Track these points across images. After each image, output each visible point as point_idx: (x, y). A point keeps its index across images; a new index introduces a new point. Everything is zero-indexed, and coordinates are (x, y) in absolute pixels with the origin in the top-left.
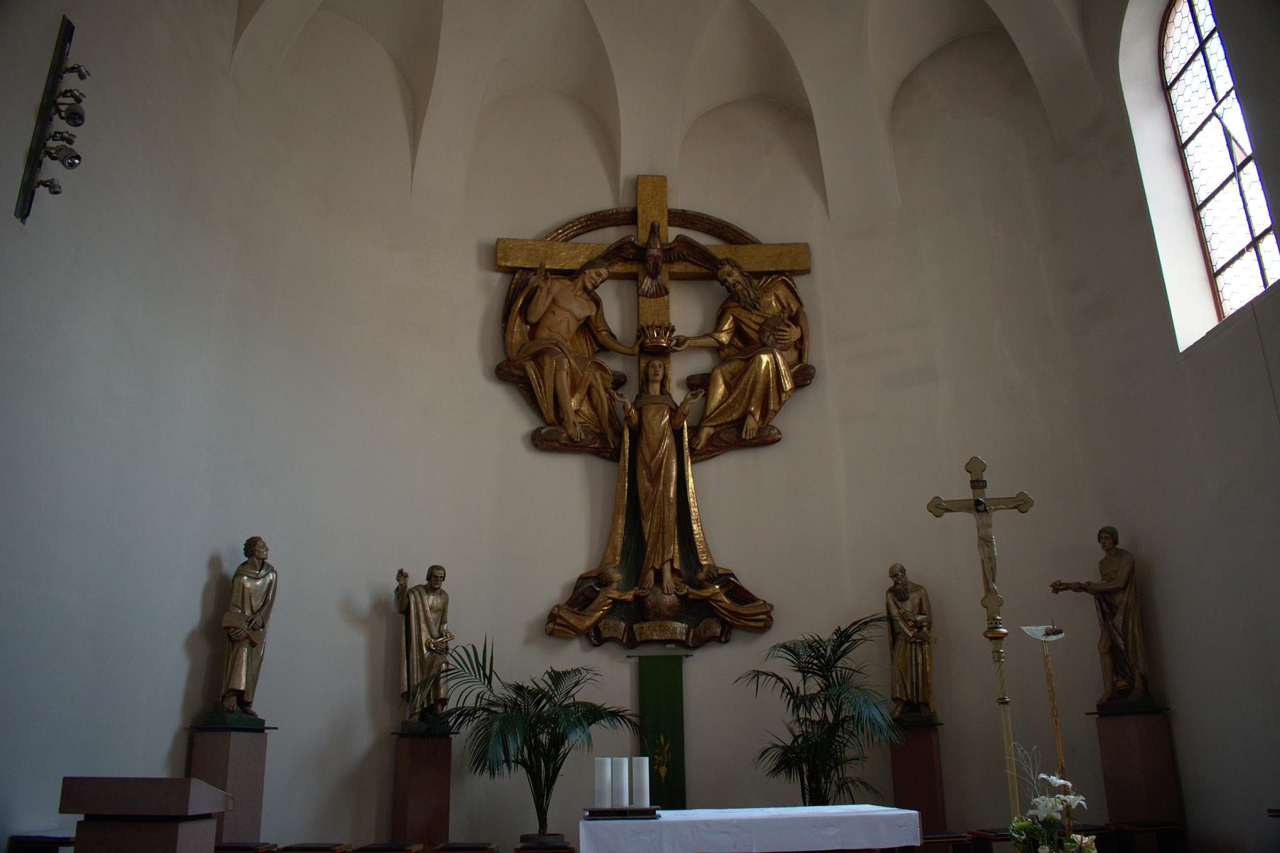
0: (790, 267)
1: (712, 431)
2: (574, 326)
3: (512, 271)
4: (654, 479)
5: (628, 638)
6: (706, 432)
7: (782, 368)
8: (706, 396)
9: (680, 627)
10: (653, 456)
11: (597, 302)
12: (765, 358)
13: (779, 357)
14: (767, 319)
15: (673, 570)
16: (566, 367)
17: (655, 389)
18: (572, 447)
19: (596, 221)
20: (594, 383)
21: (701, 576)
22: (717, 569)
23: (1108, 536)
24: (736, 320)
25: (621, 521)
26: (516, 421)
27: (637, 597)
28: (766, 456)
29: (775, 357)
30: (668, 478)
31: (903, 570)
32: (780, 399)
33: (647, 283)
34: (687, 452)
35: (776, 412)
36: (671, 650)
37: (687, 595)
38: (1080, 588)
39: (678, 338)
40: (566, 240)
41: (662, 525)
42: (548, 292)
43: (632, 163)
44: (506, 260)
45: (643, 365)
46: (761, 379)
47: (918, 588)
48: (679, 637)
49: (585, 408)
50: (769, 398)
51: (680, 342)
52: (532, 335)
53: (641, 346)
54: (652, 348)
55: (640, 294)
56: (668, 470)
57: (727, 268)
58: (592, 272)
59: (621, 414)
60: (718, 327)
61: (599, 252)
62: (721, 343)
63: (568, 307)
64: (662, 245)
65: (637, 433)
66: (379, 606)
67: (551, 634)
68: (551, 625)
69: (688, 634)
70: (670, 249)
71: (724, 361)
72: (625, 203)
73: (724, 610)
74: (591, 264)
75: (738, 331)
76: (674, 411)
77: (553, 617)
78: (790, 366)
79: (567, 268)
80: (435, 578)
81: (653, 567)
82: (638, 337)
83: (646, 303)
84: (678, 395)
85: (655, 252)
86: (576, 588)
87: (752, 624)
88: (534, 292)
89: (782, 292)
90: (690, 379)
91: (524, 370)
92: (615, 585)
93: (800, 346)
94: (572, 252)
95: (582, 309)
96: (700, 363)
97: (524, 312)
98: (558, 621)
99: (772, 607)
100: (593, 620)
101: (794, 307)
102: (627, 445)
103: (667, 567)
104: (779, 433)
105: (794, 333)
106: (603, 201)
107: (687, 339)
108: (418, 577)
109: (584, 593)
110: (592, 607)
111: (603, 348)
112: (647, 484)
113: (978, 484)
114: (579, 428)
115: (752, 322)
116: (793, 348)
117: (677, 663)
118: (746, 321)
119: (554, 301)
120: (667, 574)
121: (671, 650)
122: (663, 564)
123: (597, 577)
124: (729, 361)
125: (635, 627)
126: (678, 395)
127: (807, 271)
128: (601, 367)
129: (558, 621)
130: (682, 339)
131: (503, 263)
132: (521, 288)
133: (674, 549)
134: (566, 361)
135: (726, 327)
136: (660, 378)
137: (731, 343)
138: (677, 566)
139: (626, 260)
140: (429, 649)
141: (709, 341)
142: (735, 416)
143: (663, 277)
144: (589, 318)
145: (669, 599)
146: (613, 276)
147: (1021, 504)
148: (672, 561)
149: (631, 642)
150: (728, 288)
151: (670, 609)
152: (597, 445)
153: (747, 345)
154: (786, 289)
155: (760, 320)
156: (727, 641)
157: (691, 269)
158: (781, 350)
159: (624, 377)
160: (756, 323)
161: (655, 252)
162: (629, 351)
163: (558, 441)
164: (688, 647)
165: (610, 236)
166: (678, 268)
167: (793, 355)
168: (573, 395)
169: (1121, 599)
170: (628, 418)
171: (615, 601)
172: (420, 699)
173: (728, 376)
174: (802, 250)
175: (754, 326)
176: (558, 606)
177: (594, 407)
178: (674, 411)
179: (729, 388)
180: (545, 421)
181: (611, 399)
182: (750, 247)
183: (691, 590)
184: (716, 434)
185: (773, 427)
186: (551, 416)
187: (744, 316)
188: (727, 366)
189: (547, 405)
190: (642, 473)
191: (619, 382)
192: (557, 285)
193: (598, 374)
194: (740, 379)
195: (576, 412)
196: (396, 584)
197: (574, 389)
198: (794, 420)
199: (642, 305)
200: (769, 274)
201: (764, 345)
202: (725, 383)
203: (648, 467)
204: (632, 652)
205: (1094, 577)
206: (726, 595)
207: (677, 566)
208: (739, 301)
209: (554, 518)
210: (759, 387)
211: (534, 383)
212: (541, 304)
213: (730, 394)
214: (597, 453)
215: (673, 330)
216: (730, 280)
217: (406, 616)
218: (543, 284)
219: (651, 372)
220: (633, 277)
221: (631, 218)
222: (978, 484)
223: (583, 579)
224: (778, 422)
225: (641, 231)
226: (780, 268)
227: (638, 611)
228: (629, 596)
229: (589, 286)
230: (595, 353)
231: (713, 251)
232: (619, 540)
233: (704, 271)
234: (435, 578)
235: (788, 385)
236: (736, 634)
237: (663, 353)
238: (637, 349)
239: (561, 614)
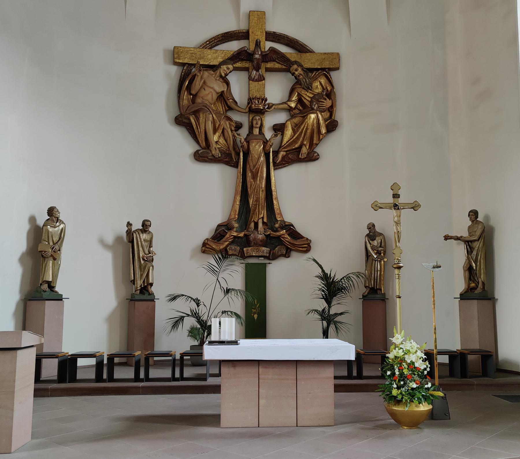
0: (328, 67)
1: (285, 153)
2: (215, 96)
3: (183, 65)
4: (254, 177)
5: (241, 254)
6: (282, 154)
7: (321, 121)
8: (283, 135)
9: (265, 250)
10: (254, 166)
11: (228, 83)
12: (313, 116)
13: (320, 115)
14: (315, 95)
15: (264, 223)
16: (211, 119)
17: (256, 131)
18: (214, 160)
20: (225, 127)
21: (277, 226)
22: (285, 222)
23: (474, 214)
24: (299, 95)
25: (238, 198)
26: (186, 146)
27: (245, 235)
28: (311, 166)
29: (317, 116)
30: (262, 177)
31: (374, 225)
32: (319, 138)
33: (254, 72)
34: (271, 165)
35: (317, 145)
36: (262, 261)
37: (269, 235)
38: (457, 238)
39: (269, 104)
40: (211, 48)
41: (257, 200)
42: (202, 78)
44: (179, 59)
45: (251, 118)
46: (310, 127)
47: (381, 234)
48: (265, 255)
49: (222, 140)
50: (315, 138)
51: (270, 106)
52: (193, 101)
53: (250, 108)
54: (257, 108)
55: (250, 79)
56: (262, 173)
57: (295, 66)
58: (224, 67)
59: (239, 145)
60: (289, 100)
61: (229, 55)
62: (291, 107)
63: (212, 86)
64: (262, 52)
65: (247, 154)
66: (118, 239)
67: (204, 252)
68: (203, 248)
69: (270, 253)
70: (266, 55)
71: (293, 117)
72: (243, 26)
73: (288, 241)
74: (224, 63)
75: (300, 101)
76: (265, 142)
77: (204, 244)
78: (325, 120)
79: (211, 64)
81: (254, 221)
82: (248, 103)
83: (253, 84)
84: (268, 134)
85: (257, 56)
86: (216, 230)
87: (301, 249)
88: (194, 76)
89: (323, 80)
90: (275, 125)
91: (189, 120)
92: (235, 229)
93: (331, 110)
94: (215, 55)
95: (219, 87)
96: (281, 118)
97: (189, 88)
98: (207, 246)
99: (310, 241)
100: (224, 246)
101: (329, 88)
102: (242, 161)
103: (260, 222)
104: (318, 155)
105: (328, 103)
106: (231, 25)
107: (273, 105)
108: (137, 225)
109: (220, 233)
110: (224, 239)
111: (230, 109)
112: (252, 180)
113: (396, 196)
114: (218, 151)
115: (307, 96)
116: (327, 111)
117: (264, 266)
118: (304, 96)
119: (204, 82)
120: (260, 225)
121: (262, 261)
122: (258, 220)
123: (226, 225)
124: (295, 117)
125: (245, 249)
126: (268, 134)
127: (337, 69)
128: (229, 119)
129: (207, 246)
130: (271, 105)
131: (177, 61)
132: (188, 75)
133: (264, 213)
134: (211, 115)
135: (294, 99)
136: (259, 126)
137: (296, 107)
138: (265, 220)
139: (242, 60)
140: (143, 259)
141: (285, 106)
142: (297, 146)
143: (262, 71)
144: (223, 92)
145: (260, 237)
146: (236, 69)
147: (415, 207)
148: (263, 218)
149: (242, 256)
150: (296, 77)
151: (261, 241)
152: (227, 160)
153: (304, 108)
154: (325, 79)
155: (311, 96)
156: (289, 257)
157: (277, 66)
158: (321, 112)
159: (241, 124)
160: (309, 97)
161: (257, 56)
162: (244, 111)
163: (207, 157)
164: (269, 259)
165: (234, 46)
166: (269, 65)
167: (327, 115)
168: (215, 133)
169: (476, 245)
170: (242, 146)
171: (235, 237)
172: (139, 283)
173: (294, 125)
174: (336, 57)
175: (308, 98)
176: (207, 239)
177: (226, 141)
179: (294, 131)
180: (200, 146)
181: (234, 136)
182: (308, 54)
183: (272, 232)
184: (287, 155)
185: (316, 152)
186: (204, 144)
187: (303, 92)
188: (294, 120)
189: (202, 139)
190: (249, 174)
191: (239, 126)
192: (206, 74)
193: (227, 123)
194: (300, 127)
195: (216, 142)
196: (127, 229)
197: (215, 131)
198: (327, 148)
199: (251, 86)
200: (317, 70)
201: (313, 109)
202: (293, 129)
203: (252, 172)
204: (243, 261)
205: (465, 234)
206: (289, 235)
207: (265, 220)
208: (301, 85)
210: (309, 131)
211: (195, 127)
212: (197, 84)
213: (294, 135)
214: (228, 163)
215: (266, 100)
216: (296, 73)
218: (199, 74)
219: (255, 122)
220: (246, 69)
221: (244, 35)
222: (396, 196)
223: (219, 226)
224: (319, 150)
225: (251, 44)
226: (323, 67)
227: (246, 241)
228: (242, 235)
229: (223, 75)
230: (226, 111)
231: (288, 56)
232: (237, 207)
233: (284, 67)
235: (324, 131)
236: (294, 254)
237: (261, 112)
238: (247, 110)
239: (209, 243)
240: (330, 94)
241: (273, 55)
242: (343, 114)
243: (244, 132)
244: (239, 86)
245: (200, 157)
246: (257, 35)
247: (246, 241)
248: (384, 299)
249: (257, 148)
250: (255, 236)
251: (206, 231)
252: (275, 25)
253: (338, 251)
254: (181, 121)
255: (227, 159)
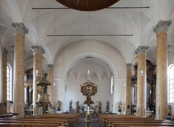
19: (86, 83)
43: (88, 80)
76: (90, 94)
80: (79, 101)
83: (89, 88)
84: (90, 93)
96: (91, 91)
106: (86, 82)
109: (85, 102)
132: (82, 88)
149: (87, 104)
153: (94, 90)
165: (87, 84)
178: (90, 94)
198: (96, 94)
209: (84, 98)
217: (78, 103)
234: (79, 101)
240: (96, 89)
241: (91, 85)
242: (98, 91)
243: (87, 92)
244: (87, 88)
245: (83, 95)
246: (89, 83)
247: (88, 103)
248: (101, 108)
249: (89, 94)
250: (89, 102)
251: (84, 102)
252: (91, 82)
253: (96, 104)
254: (82, 92)
255: (86, 95)
